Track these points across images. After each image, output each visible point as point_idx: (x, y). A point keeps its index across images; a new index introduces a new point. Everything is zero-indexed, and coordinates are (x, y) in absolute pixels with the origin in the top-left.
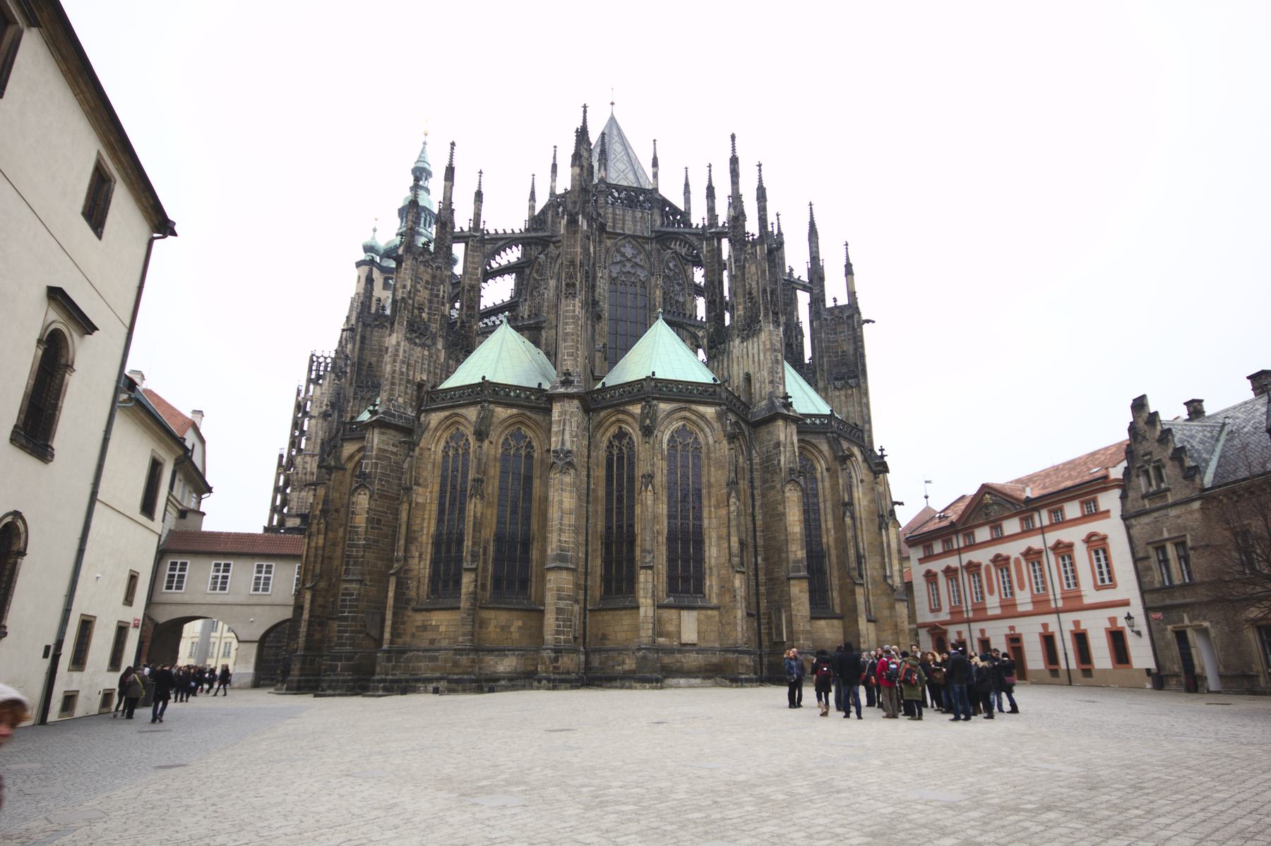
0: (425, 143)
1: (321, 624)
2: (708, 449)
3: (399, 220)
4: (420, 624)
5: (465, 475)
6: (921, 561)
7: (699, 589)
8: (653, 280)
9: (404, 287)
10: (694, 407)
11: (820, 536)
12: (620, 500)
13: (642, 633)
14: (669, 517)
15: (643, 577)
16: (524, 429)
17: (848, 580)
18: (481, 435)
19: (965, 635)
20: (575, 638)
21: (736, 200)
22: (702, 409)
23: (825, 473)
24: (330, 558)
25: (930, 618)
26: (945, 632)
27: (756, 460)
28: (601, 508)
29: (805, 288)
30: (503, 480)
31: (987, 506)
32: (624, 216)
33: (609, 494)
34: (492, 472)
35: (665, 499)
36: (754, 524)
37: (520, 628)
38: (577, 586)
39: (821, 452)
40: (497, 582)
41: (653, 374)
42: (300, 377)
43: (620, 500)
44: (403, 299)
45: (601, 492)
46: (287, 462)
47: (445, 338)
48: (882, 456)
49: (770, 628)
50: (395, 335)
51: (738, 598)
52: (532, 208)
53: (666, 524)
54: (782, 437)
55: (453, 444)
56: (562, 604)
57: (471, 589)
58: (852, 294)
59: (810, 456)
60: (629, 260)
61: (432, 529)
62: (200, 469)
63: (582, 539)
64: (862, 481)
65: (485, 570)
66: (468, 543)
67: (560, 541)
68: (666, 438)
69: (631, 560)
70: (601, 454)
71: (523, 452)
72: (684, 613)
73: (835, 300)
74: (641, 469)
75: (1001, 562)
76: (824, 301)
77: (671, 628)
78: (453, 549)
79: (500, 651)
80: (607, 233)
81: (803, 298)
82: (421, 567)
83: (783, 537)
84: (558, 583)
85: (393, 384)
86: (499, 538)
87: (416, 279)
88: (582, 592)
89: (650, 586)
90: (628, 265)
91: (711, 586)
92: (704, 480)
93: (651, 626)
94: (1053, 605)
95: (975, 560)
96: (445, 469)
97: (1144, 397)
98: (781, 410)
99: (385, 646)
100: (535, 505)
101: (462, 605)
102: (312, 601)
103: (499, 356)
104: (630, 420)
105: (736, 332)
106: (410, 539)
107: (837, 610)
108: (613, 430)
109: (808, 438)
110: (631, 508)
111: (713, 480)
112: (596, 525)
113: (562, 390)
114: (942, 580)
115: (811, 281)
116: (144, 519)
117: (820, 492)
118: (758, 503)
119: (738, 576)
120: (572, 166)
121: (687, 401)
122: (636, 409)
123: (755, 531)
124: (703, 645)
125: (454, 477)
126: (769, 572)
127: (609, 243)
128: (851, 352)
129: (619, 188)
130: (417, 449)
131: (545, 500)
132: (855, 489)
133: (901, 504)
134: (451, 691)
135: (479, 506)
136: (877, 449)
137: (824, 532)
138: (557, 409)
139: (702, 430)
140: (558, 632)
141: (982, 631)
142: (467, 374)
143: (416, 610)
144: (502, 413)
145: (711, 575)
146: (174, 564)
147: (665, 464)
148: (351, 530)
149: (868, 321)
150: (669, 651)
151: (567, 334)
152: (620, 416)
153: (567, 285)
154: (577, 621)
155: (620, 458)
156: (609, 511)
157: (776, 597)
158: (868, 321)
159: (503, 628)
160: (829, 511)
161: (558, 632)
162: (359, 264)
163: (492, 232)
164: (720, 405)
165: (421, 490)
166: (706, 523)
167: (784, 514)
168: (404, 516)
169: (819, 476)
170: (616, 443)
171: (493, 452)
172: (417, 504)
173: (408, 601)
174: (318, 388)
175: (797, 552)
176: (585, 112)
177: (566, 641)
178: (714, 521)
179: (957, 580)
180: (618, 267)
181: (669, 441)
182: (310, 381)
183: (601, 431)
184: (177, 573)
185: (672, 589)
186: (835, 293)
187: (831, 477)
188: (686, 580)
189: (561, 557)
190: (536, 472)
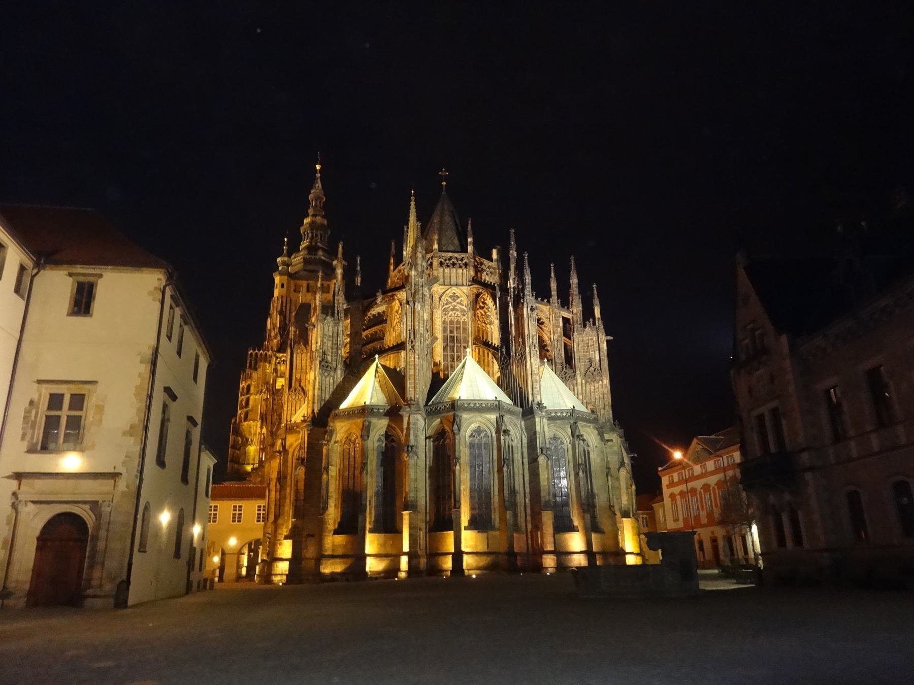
9: (317, 343)
75: (706, 487)
147: (467, 451)
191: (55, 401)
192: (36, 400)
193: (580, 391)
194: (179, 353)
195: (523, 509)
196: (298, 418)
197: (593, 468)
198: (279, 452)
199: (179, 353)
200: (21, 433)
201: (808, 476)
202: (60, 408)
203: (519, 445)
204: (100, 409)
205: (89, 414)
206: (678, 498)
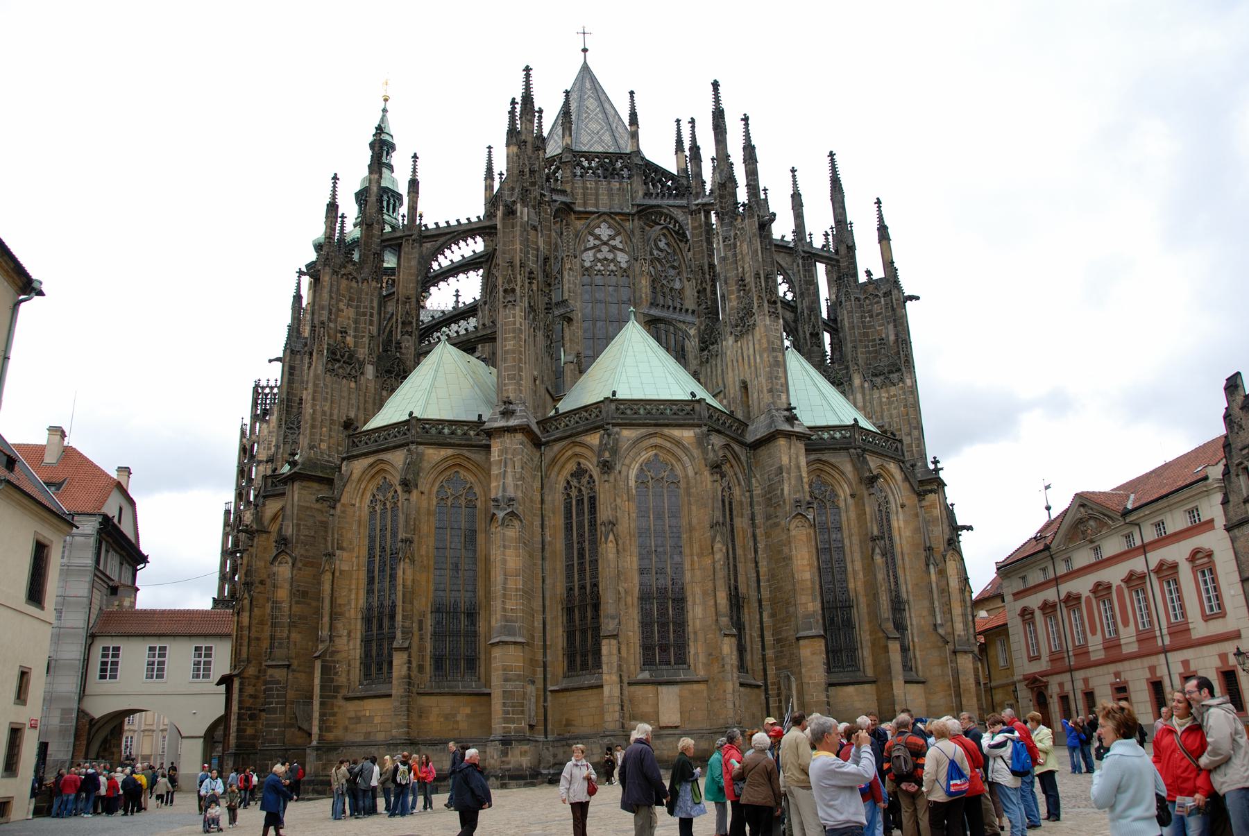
0: (385, 110)
1: (252, 717)
2: (688, 483)
4: (352, 714)
5: (394, 534)
6: (1017, 595)
7: (682, 659)
8: (637, 265)
10: (666, 431)
11: (846, 581)
12: (581, 555)
13: (608, 717)
14: (642, 571)
15: (608, 648)
16: (462, 472)
17: (881, 635)
18: (407, 485)
19: (1068, 687)
20: (531, 727)
21: (722, 159)
23: (850, 500)
24: (258, 639)
26: (1046, 685)
27: (757, 491)
28: (560, 565)
32: (597, 189)
33: (569, 547)
34: (424, 528)
35: (635, 550)
36: (758, 572)
37: (468, 716)
38: (532, 661)
39: (842, 473)
40: (438, 661)
41: (614, 393)
42: (244, 412)
43: (581, 555)
45: (560, 545)
46: (235, 518)
47: (377, 365)
48: (937, 470)
49: (780, 701)
51: (728, 667)
52: (489, 188)
53: (636, 580)
54: (785, 460)
55: (380, 497)
56: (509, 686)
57: (404, 671)
58: (889, 264)
59: (829, 480)
60: (605, 243)
61: (362, 602)
62: (131, 536)
63: (537, 604)
64: (903, 506)
65: (421, 649)
66: (399, 617)
67: (504, 609)
68: (633, 474)
69: (597, 629)
70: (556, 498)
71: (463, 501)
72: (663, 690)
73: (869, 273)
74: (604, 514)
75: (1101, 590)
76: (855, 275)
78: (386, 624)
80: (575, 212)
83: (790, 587)
84: (504, 663)
85: (313, 427)
86: (437, 610)
88: (540, 670)
89: (615, 659)
90: (605, 249)
91: (696, 654)
92: (684, 522)
93: (618, 708)
94: (1160, 643)
96: (372, 529)
97: (1238, 374)
98: (786, 426)
99: (314, 743)
100: (480, 566)
101: (394, 692)
102: (241, 690)
103: (433, 385)
105: (728, 329)
106: (334, 616)
107: (870, 673)
108: (571, 466)
109: (826, 456)
110: (595, 562)
111: (694, 521)
112: (554, 586)
113: (501, 423)
115: (837, 251)
117: (845, 526)
118: (761, 546)
119: (727, 640)
120: (508, 145)
121: (656, 425)
122: (594, 439)
123: (758, 581)
124: (688, 727)
125: (383, 537)
126: (777, 631)
127: (579, 224)
128: (892, 338)
129: (589, 156)
130: (339, 506)
131: (487, 560)
132: (893, 517)
133: (969, 528)
135: (409, 572)
136: (930, 459)
137: (850, 576)
138: (496, 446)
139: (679, 460)
140: (506, 720)
141: (1086, 681)
142: (393, 412)
143: (347, 699)
144: (434, 455)
145: (696, 640)
146: (106, 649)
147: (633, 507)
148: (276, 605)
149: (911, 298)
151: (506, 352)
152: (578, 449)
153: (505, 291)
154: (531, 706)
156: (569, 568)
157: (785, 662)
158: (911, 298)
159: (447, 717)
160: (856, 548)
161: (506, 720)
163: (431, 226)
164: (700, 426)
165: (345, 554)
166: (688, 575)
167: (790, 558)
168: (327, 587)
169: (842, 504)
170: (574, 483)
171: (424, 504)
172: (341, 572)
173: (337, 689)
174: (265, 426)
175: (809, 605)
176: (528, 76)
177: (516, 730)
178: (698, 573)
179: (1056, 617)
180: (591, 253)
181: (637, 477)
182: (255, 418)
183: (556, 469)
184: (110, 660)
185: (648, 662)
186: (868, 261)
187: (857, 505)
188: (664, 649)
190: (480, 525)
195: (756, 634)
197: (898, 549)
203: (746, 500)
206: (1038, 614)
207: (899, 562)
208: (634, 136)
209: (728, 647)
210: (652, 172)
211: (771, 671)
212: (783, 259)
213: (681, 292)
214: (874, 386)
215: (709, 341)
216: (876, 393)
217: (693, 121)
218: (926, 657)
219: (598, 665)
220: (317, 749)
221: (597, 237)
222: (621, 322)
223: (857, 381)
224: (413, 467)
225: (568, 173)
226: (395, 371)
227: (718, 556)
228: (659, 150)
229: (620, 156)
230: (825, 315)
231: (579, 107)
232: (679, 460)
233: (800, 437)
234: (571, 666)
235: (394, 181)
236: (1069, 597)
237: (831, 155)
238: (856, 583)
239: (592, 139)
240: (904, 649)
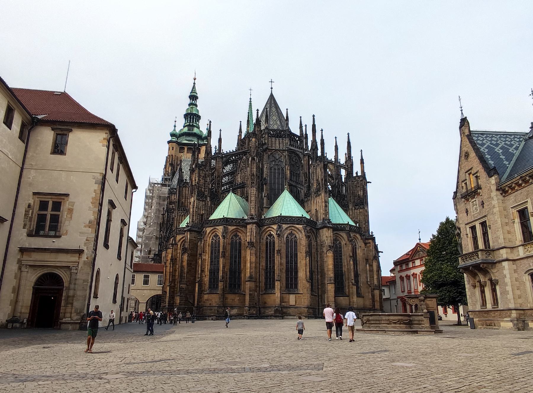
0: (194, 83)
3: (184, 120)
7: (296, 287)
9: (196, 180)
15: (277, 284)
21: (314, 141)
22: (297, 226)
25: (401, 295)
29: (345, 168)
30: (231, 251)
31: (418, 252)
38: (256, 286)
44: (195, 185)
50: (193, 198)
52: (240, 135)
65: (226, 281)
66: (221, 274)
68: (285, 236)
73: (357, 173)
76: (352, 174)
77: (286, 300)
79: (232, 307)
81: (343, 172)
82: (206, 279)
87: (199, 176)
89: (279, 287)
95: (415, 273)
98: (327, 224)
100: (242, 259)
104: (272, 230)
105: (313, 193)
106: (202, 271)
107: (347, 294)
113: (251, 221)
114: (405, 279)
116: (130, 269)
122: (275, 227)
127: (269, 153)
132: (357, 250)
134: (217, 319)
136: (370, 232)
144: (231, 228)
147: (285, 246)
148: (182, 266)
149: (369, 182)
150: (287, 307)
152: (270, 229)
155: (270, 243)
158: (369, 182)
162: (169, 142)
163: (225, 153)
166: (299, 265)
170: (269, 238)
175: (330, 274)
185: (287, 287)
186: (357, 169)
189: (251, 277)
190: (242, 248)
191: (43, 205)
192: (32, 204)
193: (351, 214)
194: (117, 181)
196: (183, 225)
197: (358, 259)
198: (172, 245)
199: (117, 181)
200: (23, 223)
201: (505, 264)
202: (46, 209)
203: (315, 244)
204: (71, 211)
205: (64, 214)
206: (405, 278)
207: (358, 262)
208: (287, 124)
209: (308, 285)
210: (291, 135)
211: (320, 292)
212: (330, 166)
213: (299, 174)
214: (355, 209)
215: (308, 195)
216: (356, 211)
217: (306, 126)
218: (364, 290)
219: (274, 288)
220: (197, 307)
221: (275, 158)
222: (283, 191)
223: (350, 207)
224: (225, 231)
225: (267, 136)
226: (217, 200)
227: (308, 260)
228: (295, 129)
229: (283, 131)
230: (343, 180)
231: (270, 110)
232: (297, 233)
233: (331, 228)
234: (266, 289)
235: (198, 111)
236: (413, 274)
237: (348, 134)
238: (345, 269)
239: (275, 125)
240: (358, 288)
